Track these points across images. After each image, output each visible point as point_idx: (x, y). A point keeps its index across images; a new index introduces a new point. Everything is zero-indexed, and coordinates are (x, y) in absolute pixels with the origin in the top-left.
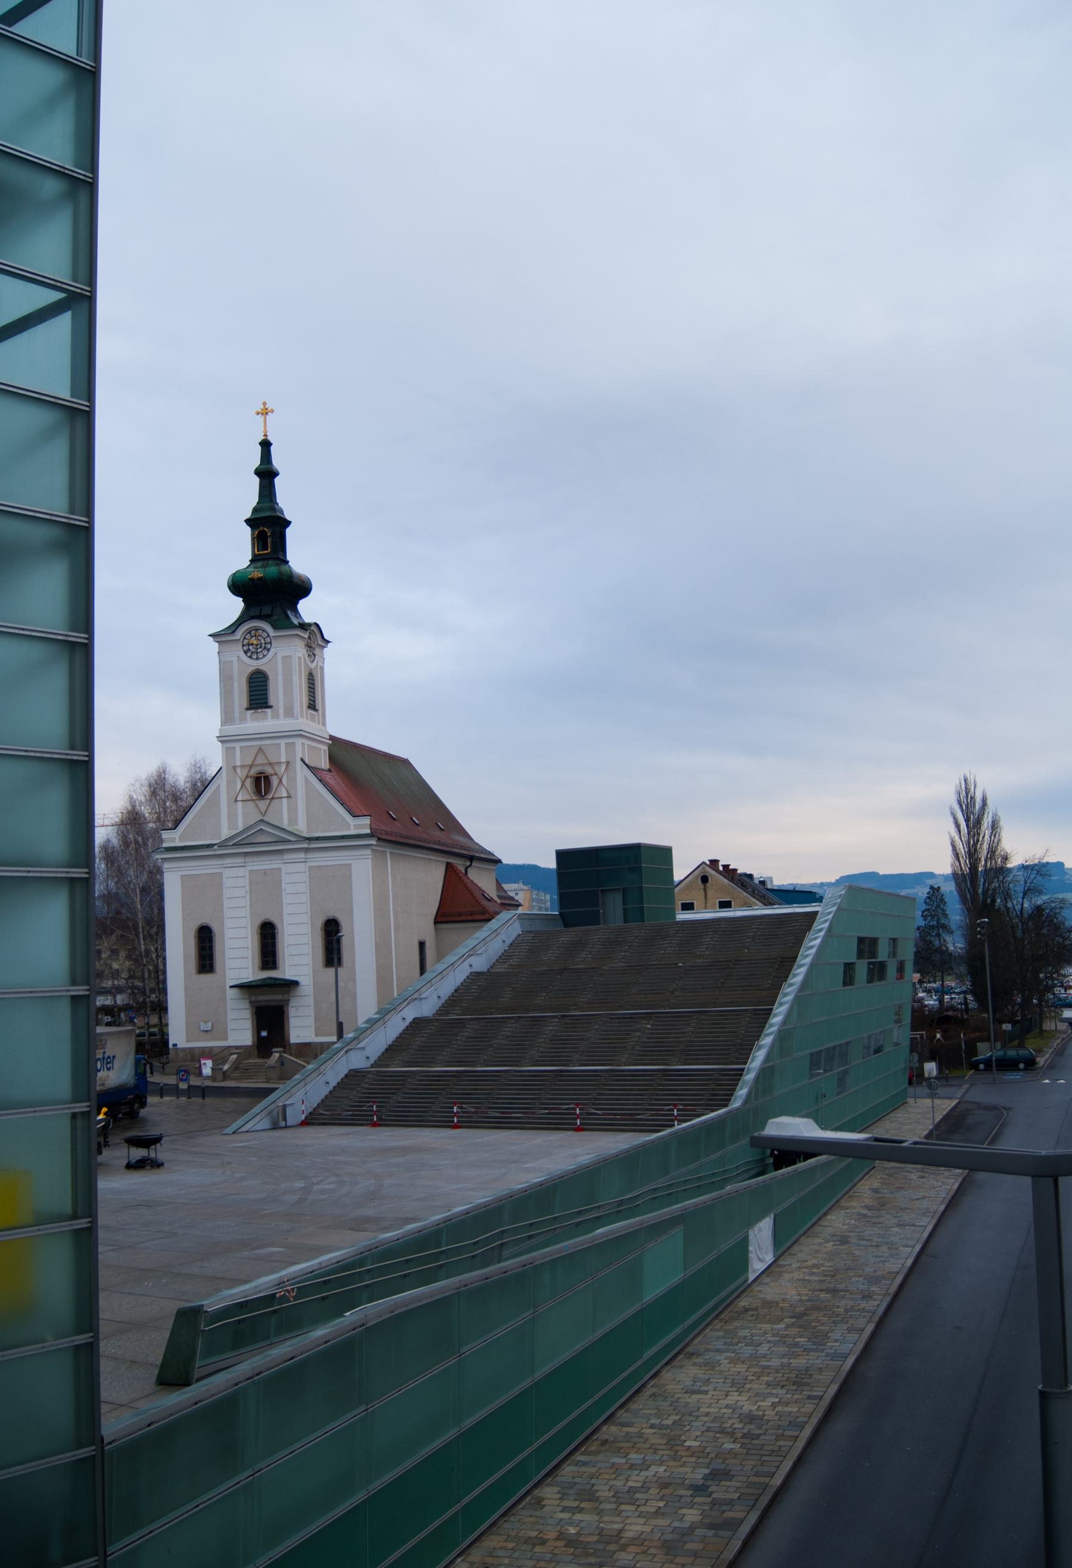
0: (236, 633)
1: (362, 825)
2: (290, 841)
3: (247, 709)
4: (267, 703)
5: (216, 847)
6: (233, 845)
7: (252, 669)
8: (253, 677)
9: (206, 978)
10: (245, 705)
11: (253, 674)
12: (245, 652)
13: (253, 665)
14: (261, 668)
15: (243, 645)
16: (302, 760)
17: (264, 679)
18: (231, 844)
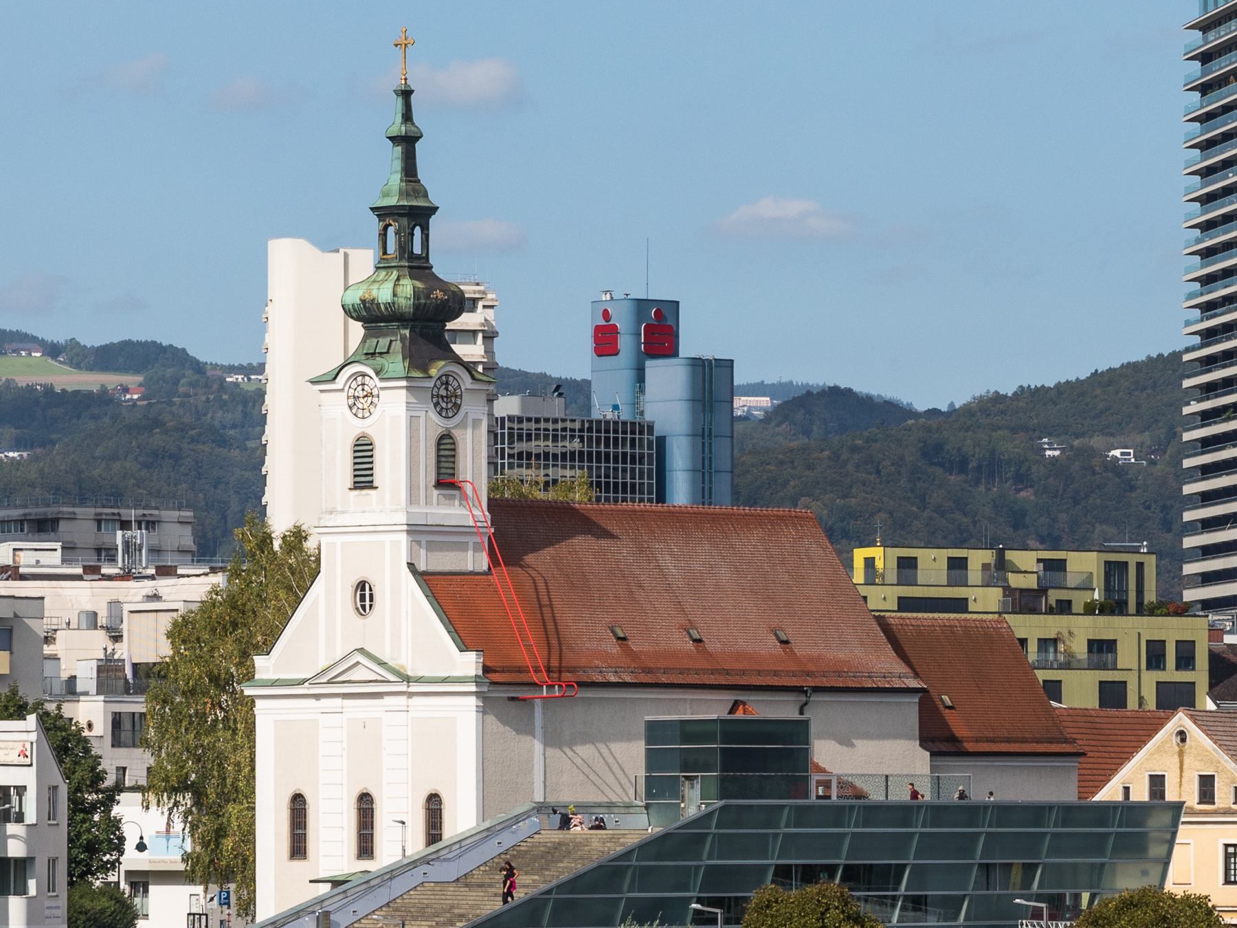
0: (337, 380)
1: (469, 664)
2: (389, 682)
3: (350, 489)
4: (372, 482)
5: (306, 684)
6: (329, 682)
7: (356, 432)
8: (358, 443)
9: (297, 864)
10: (349, 481)
11: (358, 440)
12: (350, 408)
13: (358, 427)
14: (365, 430)
15: (348, 397)
16: (411, 566)
17: (370, 447)
18: (325, 680)
